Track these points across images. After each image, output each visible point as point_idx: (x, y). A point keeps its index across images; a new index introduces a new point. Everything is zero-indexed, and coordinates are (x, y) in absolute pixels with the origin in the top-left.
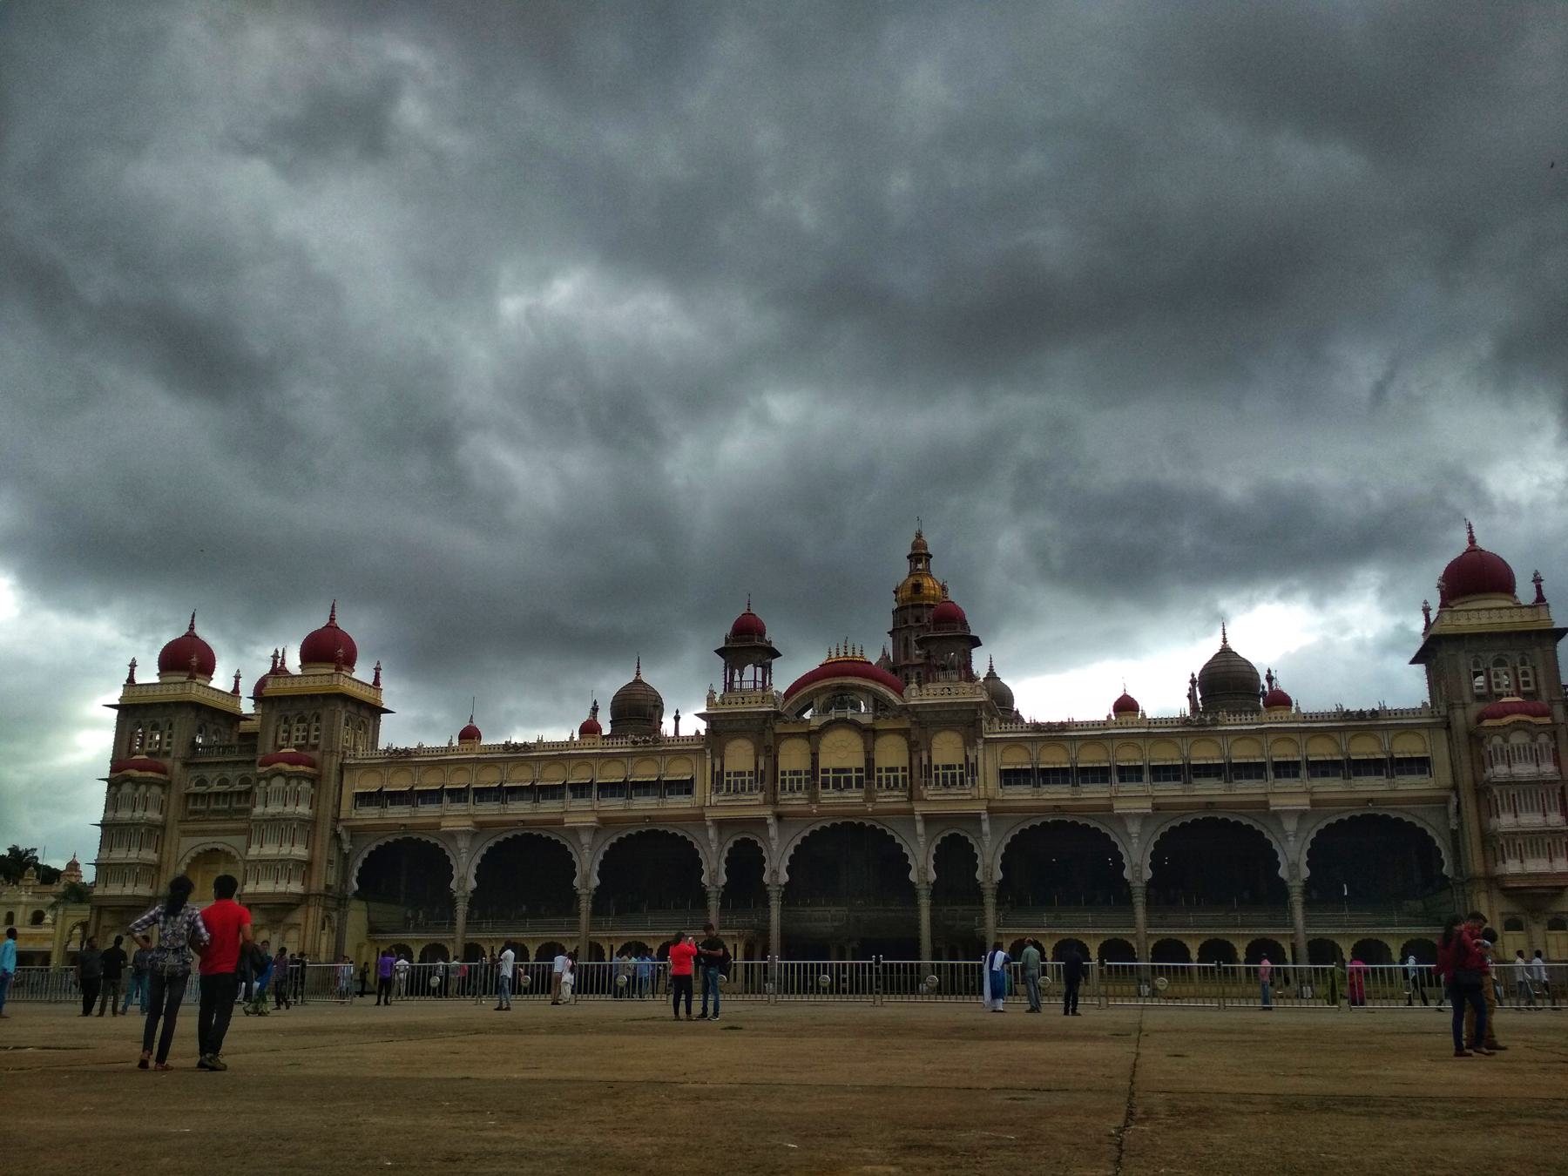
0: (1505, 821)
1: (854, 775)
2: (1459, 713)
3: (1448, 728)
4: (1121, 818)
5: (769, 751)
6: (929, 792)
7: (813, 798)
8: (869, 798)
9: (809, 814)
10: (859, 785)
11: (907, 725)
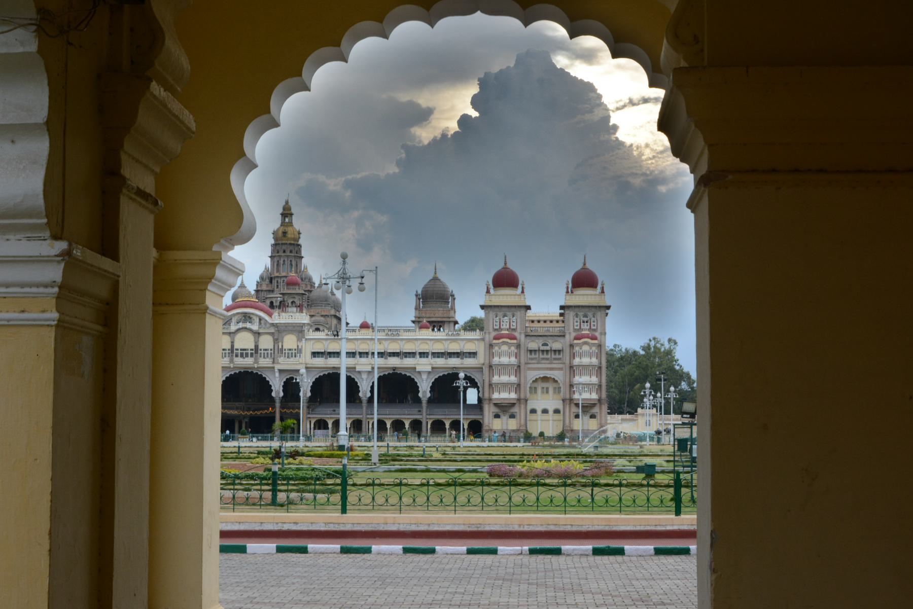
1: (249, 352)
2: (487, 336)
3: (483, 339)
6: (281, 360)
7: (232, 361)
10: (252, 355)
11: (272, 330)
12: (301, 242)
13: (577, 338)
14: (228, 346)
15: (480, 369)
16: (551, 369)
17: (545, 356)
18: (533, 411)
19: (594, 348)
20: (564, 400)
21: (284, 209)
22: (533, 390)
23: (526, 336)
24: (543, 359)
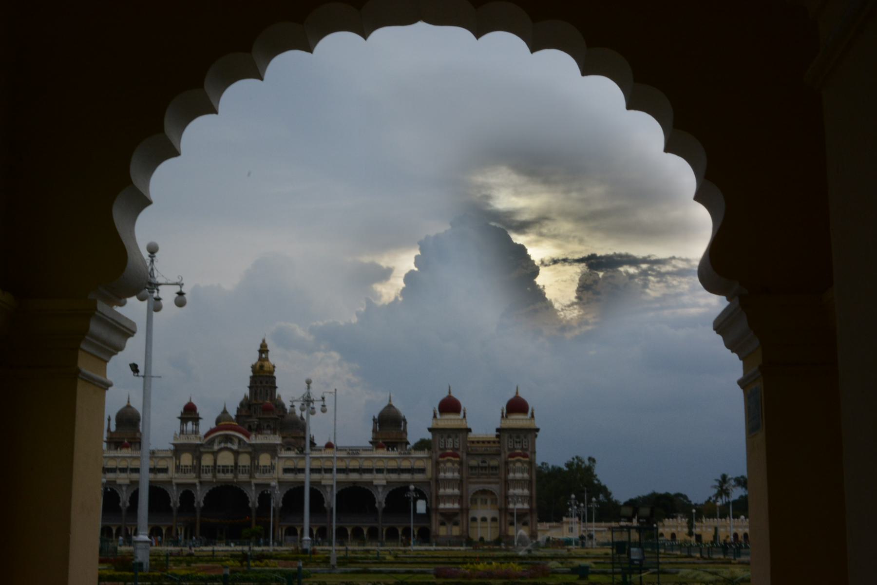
0: (442, 491)
3: (430, 458)
4: (325, 486)
5: (198, 458)
6: (257, 475)
7: (214, 476)
8: (236, 477)
9: (212, 482)
10: (232, 471)
11: (250, 450)
12: (275, 374)
13: (511, 456)
14: (211, 463)
15: (427, 483)
16: (490, 483)
17: (484, 472)
18: (474, 519)
19: (525, 465)
20: (500, 510)
21: (262, 346)
22: (474, 501)
23: (468, 454)
24: (482, 474)
